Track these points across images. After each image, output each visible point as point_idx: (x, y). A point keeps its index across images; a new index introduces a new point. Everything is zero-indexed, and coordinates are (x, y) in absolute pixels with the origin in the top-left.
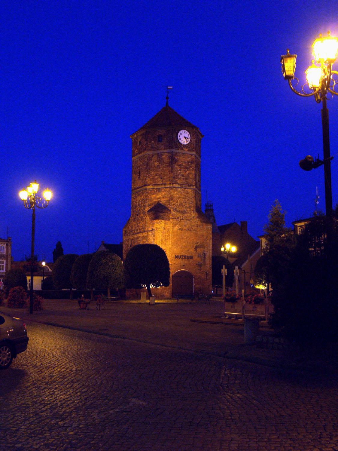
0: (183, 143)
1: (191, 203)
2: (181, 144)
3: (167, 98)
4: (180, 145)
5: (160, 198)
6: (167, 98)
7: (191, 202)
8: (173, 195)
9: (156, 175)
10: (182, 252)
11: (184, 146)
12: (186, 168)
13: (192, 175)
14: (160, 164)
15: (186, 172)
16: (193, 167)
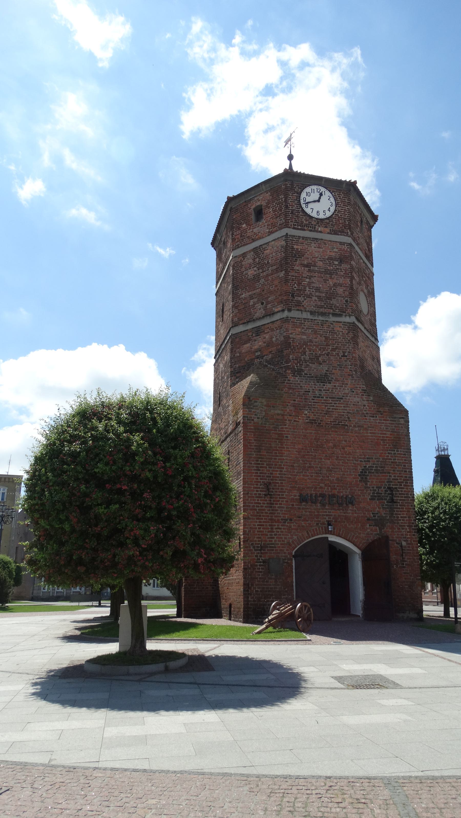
1: (344, 356)
2: (311, 217)
4: (306, 220)
5: (260, 351)
7: (344, 353)
8: (291, 336)
9: (251, 297)
10: (322, 485)
11: (320, 221)
12: (327, 272)
14: (261, 271)
15: (326, 282)
16: (346, 270)
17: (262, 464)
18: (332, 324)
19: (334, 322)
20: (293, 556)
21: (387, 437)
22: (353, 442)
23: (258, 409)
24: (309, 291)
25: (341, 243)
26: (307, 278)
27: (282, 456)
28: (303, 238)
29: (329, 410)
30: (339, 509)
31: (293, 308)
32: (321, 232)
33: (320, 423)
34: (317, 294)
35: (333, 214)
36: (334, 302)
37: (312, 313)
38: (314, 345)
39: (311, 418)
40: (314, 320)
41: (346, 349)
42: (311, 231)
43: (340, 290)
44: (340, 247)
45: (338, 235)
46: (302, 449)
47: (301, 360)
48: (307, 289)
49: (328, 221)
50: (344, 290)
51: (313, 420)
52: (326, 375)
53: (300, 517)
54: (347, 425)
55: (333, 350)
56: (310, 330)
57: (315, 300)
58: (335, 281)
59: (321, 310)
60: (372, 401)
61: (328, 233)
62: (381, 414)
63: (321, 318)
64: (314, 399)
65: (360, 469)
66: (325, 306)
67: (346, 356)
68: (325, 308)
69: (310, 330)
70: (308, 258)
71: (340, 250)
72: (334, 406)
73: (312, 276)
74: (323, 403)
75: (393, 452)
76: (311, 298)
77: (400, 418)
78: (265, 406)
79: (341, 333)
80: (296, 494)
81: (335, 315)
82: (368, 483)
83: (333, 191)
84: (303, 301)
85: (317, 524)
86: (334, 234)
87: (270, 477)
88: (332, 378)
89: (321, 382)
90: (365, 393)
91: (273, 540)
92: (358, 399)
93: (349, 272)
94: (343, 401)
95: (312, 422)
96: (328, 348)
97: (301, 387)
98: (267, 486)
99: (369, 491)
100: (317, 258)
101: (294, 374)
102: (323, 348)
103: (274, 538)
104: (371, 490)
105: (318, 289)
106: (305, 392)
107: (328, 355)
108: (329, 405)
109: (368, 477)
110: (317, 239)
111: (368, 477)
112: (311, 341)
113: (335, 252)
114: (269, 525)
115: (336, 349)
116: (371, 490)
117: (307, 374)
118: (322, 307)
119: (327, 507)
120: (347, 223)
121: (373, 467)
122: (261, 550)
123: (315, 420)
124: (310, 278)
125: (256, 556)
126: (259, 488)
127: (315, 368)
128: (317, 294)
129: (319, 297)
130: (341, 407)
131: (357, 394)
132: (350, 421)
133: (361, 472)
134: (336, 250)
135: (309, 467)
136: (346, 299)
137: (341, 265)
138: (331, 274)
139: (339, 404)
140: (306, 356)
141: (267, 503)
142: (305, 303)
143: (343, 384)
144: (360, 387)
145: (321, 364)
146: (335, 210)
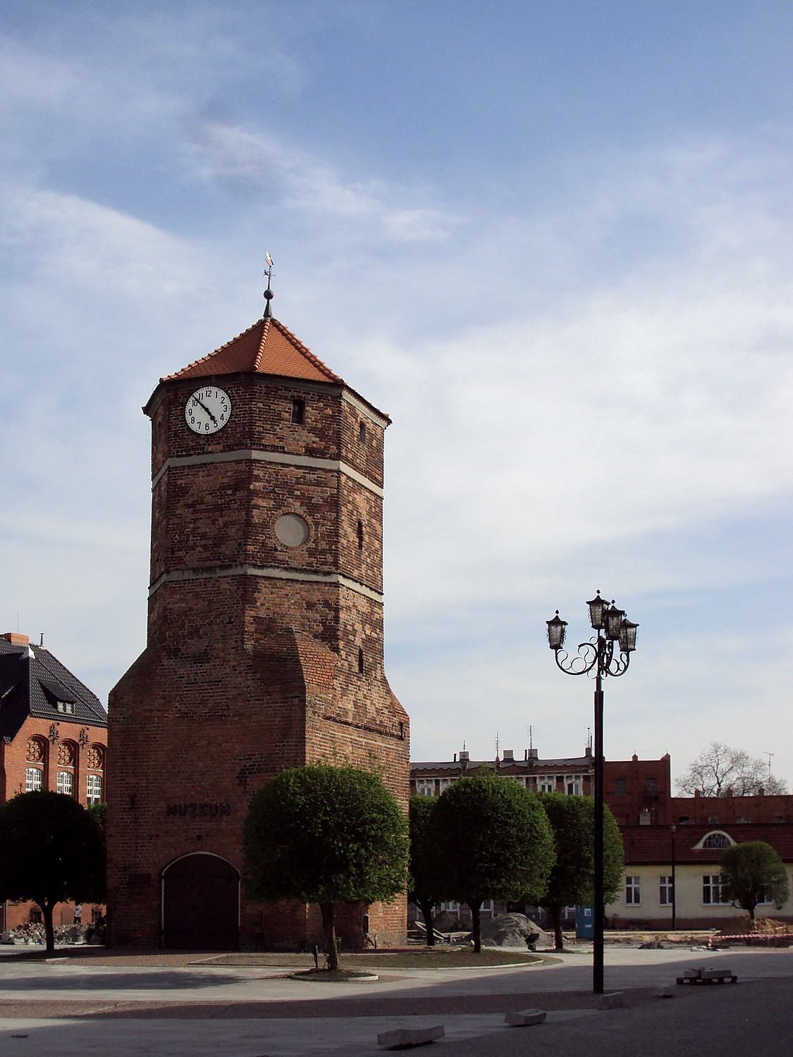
0: (202, 431)
1: (230, 622)
2: (199, 435)
3: (268, 295)
4: (192, 441)
6: (268, 295)
7: (230, 618)
10: (193, 792)
11: (210, 438)
13: (238, 527)
15: (214, 524)
17: (127, 773)
18: (218, 581)
19: (219, 577)
20: (164, 877)
21: (275, 725)
22: (232, 736)
23: (123, 707)
24: (192, 540)
25: (238, 462)
26: (190, 523)
27: (149, 762)
28: (189, 467)
29: (204, 698)
30: (211, 822)
31: (172, 568)
32: (211, 452)
33: (193, 717)
34: (203, 542)
35: (228, 421)
36: (223, 548)
37: (195, 570)
38: (195, 614)
39: (182, 711)
40: (196, 579)
41: (233, 613)
42: (199, 454)
43: (232, 531)
44: (235, 467)
45: (235, 450)
46: (172, 750)
47: (178, 636)
48: (191, 538)
49: (221, 434)
50: (237, 530)
51: (184, 713)
52: (205, 653)
53: (166, 833)
54: (225, 716)
55: (217, 616)
56: (191, 595)
57: (200, 552)
58: (226, 519)
59: (208, 564)
60: (257, 679)
61: (221, 452)
62: (269, 695)
63: (205, 575)
64: (186, 687)
65: (238, 769)
66: (212, 558)
67: (232, 622)
68: (211, 560)
69: (191, 595)
70: (193, 495)
71: (236, 471)
72: (209, 692)
73: (198, 519)
74: (197, 690)
75: (281, 744)
76: (195, 550)
77: (294, 697)
78: (132, 702)
79: (228, 592)
80: (163, 804)
81: (222, 567)
82: (248, 787)
83: (229, 389)
84: (184, 557)
85: (186, 840)
86: (229, 451)
87: (135, 787)
88: (212, 655)
89: (199, 663)
90: (250, 669)
91: (138, 860)
92: (240, 680)
93: (245, 502)
94: (223, 685)
95: (184, 716)
96: (211, 615)
97: (175, 672)
98: (133, 798)
99: (248, 797)
100: (205, 491)
101: (169, 656)
102: (204, 616)
103: (138, 857)
104: (250, 795)
105: (204, 536)
106: (179, 678)
107: (210, 625)
108: (204, 692)
109: (248, 779)
110: (206, 464)
111: (248, 779)
112: (191, 609)
113: (229, 477)
114: (135, 843)
115: (221, 614)
116: (250, 795)
117: (183, 654)
118: (207, 559)
119: (197, 819)
120: (247, 430)
121: (255, 765)
122: (124, 871)
123: (186, 713)
124: (194, 523)
125: (120, 878)
126: (124, 801)
127: (193, 645)
128: (203, 542)
129: (204, 547)
130: (219, 692)
131: (240, 673)
132: (230, 709)
133: (240, 774)
134: (229, 474)
135: (179, 772)
136: (239, 541)
137: (235, 495)
138: (222, 510)
139: (216, 688)
140: (185, 629)
141: (132, 818)
142: (187, 558)
143: (224, 661)
144: (244, 663)
145: (201, 638)
146: (231, 415)
